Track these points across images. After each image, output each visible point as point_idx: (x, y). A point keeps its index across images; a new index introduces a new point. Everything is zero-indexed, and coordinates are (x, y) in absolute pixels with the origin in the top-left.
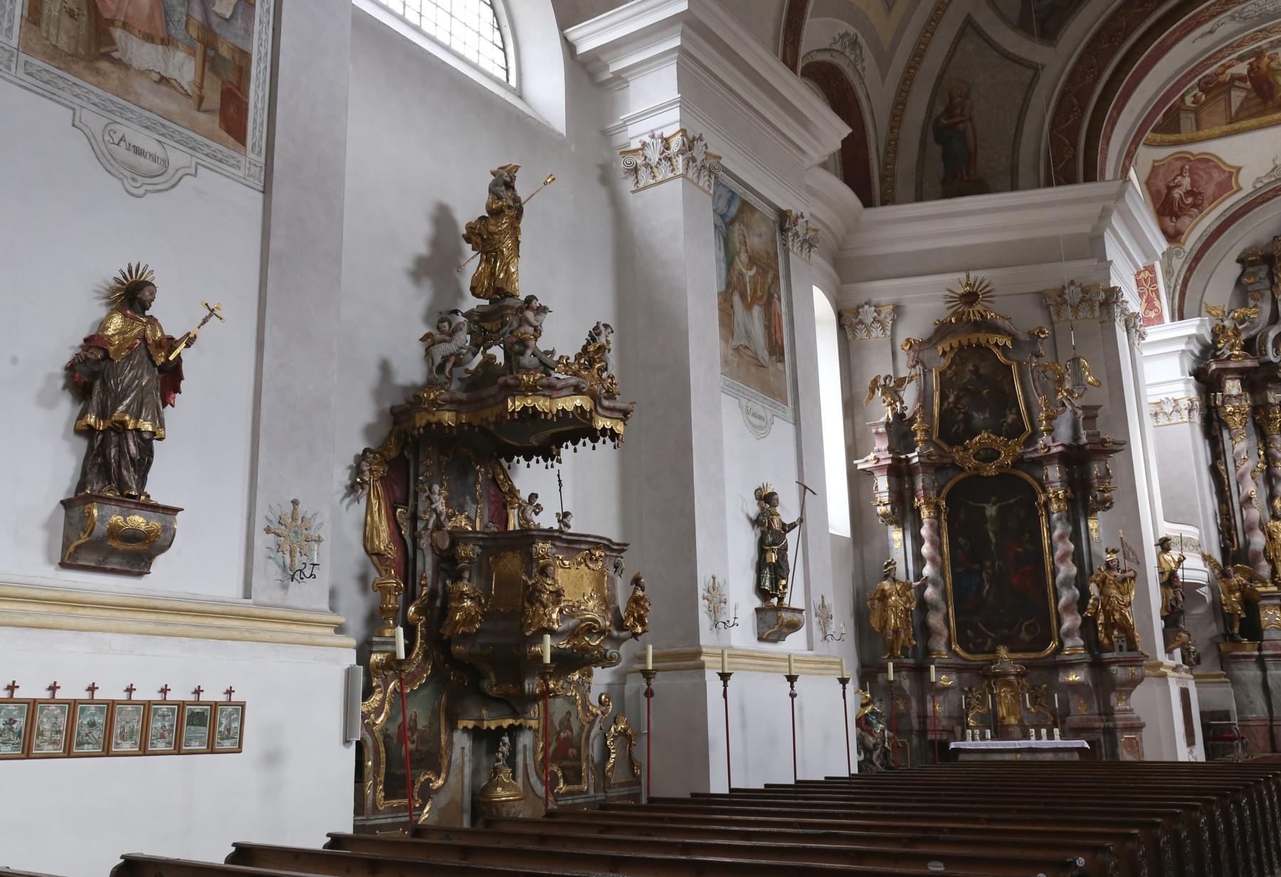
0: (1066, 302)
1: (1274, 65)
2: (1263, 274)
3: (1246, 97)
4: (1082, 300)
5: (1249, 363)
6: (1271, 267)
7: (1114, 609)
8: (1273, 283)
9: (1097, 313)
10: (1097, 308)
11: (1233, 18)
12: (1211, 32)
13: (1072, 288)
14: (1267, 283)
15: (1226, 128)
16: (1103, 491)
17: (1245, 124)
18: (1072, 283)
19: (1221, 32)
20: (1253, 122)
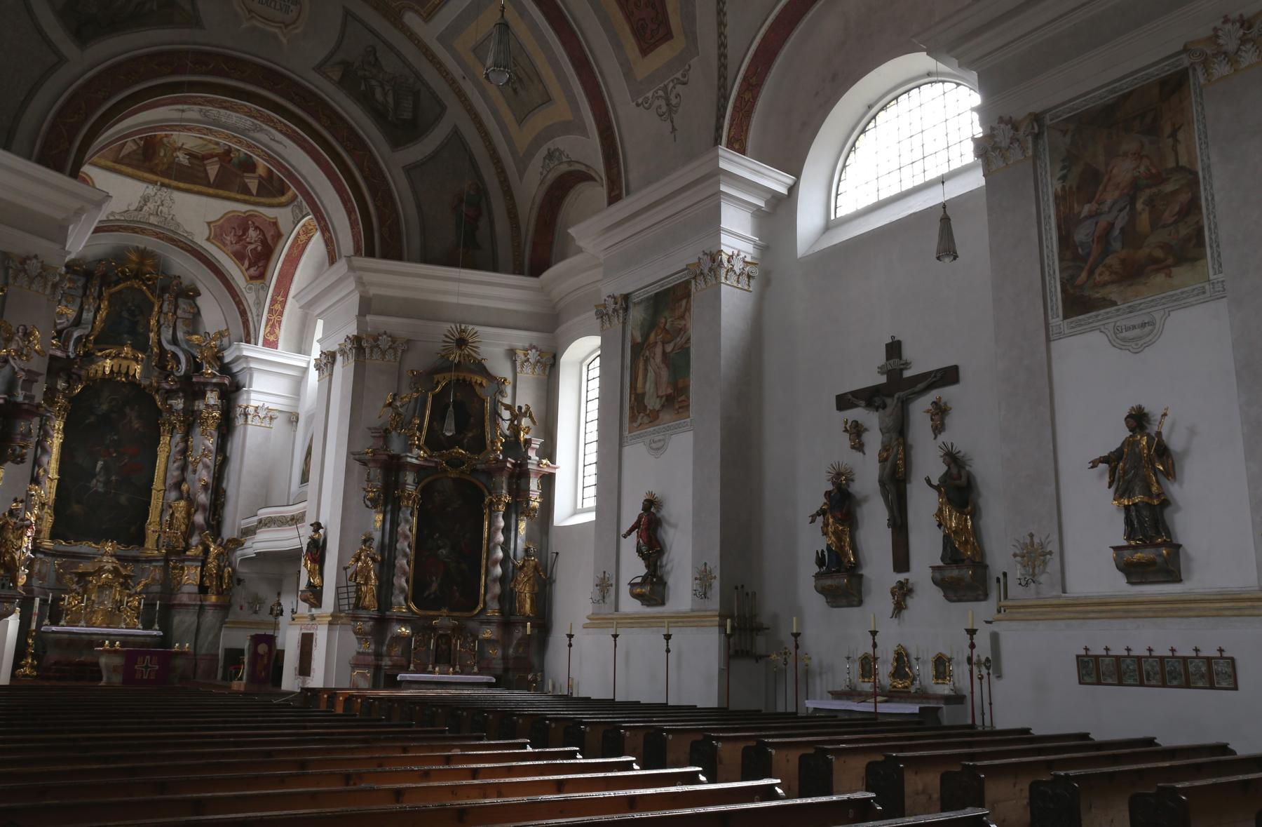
0: (25, 271)
1: (165, 140)
2: (80, 284)
3: (134, 151)
4: (40, 275)
5: (59, 353)
6: (87, 281)
7: (7, 551)
8: (85, 294)
9: (48, 291)
10: (49, 287)
11: (201, 111)
12: (183, 111)
13: (34, 261)
14: (81, 292)
15: (110, 164)
16: (23, 447)
17: (123, 168)
18: (36, 257)
19: (185, 115)
20: (129, 170)
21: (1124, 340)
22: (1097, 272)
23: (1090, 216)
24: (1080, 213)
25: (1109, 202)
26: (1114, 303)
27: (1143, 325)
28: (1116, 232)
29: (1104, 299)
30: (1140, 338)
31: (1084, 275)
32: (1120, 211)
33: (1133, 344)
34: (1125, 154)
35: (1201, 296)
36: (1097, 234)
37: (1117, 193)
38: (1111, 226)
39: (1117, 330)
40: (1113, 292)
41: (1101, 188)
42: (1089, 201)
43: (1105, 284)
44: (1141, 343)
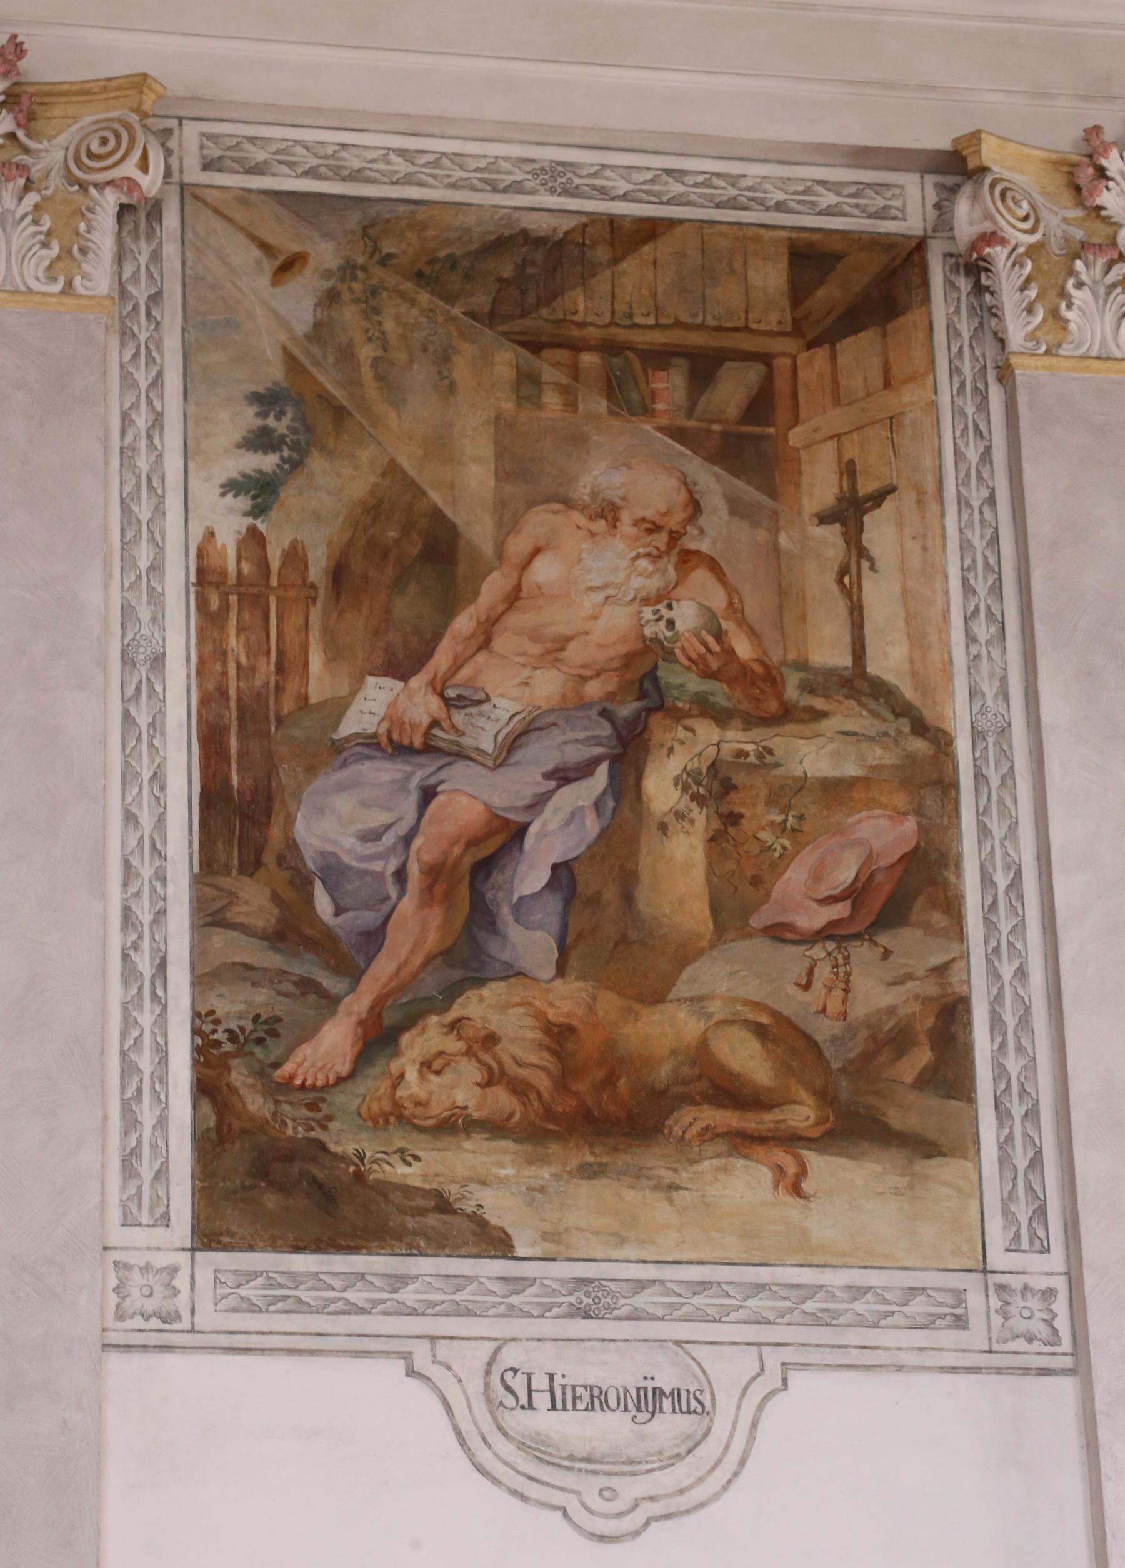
21: (538, 1449)
22: (416, 1045)
23: (393, 744)
24: (338, 708)
25: (504, 709)
26: (498, 1244)
27: (649, 1400)
28: (531, 876)
29: (443, 1205)
30: (631, 1465)
31: (333, 1043)
32: (563, 776)
33: (590, 1487)
34: (608, 513)
35: (948, 1337)
36: (425, 849)
37: (548, 686)
38: (506, 837)
39: (508, 1390)
40: (494, 1179)
41: (464, 623)
42: (400, 666)
43: (452, 1126)
44: (631, 1489)
